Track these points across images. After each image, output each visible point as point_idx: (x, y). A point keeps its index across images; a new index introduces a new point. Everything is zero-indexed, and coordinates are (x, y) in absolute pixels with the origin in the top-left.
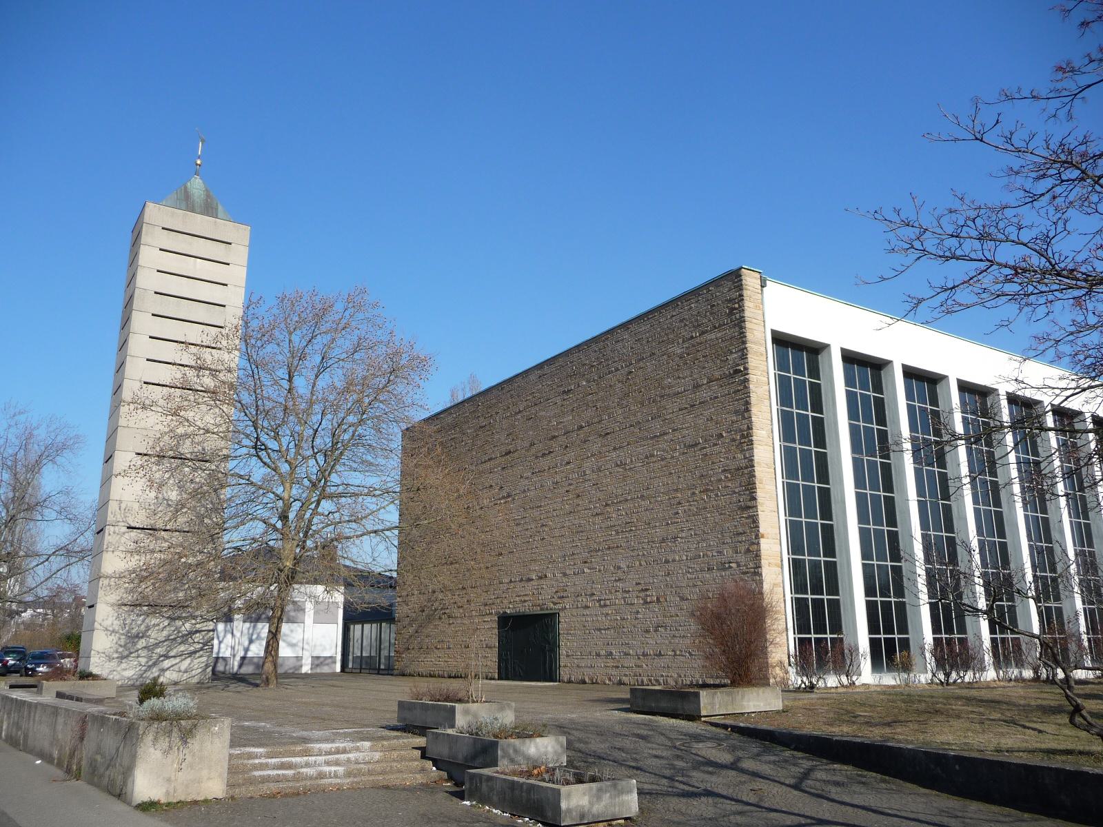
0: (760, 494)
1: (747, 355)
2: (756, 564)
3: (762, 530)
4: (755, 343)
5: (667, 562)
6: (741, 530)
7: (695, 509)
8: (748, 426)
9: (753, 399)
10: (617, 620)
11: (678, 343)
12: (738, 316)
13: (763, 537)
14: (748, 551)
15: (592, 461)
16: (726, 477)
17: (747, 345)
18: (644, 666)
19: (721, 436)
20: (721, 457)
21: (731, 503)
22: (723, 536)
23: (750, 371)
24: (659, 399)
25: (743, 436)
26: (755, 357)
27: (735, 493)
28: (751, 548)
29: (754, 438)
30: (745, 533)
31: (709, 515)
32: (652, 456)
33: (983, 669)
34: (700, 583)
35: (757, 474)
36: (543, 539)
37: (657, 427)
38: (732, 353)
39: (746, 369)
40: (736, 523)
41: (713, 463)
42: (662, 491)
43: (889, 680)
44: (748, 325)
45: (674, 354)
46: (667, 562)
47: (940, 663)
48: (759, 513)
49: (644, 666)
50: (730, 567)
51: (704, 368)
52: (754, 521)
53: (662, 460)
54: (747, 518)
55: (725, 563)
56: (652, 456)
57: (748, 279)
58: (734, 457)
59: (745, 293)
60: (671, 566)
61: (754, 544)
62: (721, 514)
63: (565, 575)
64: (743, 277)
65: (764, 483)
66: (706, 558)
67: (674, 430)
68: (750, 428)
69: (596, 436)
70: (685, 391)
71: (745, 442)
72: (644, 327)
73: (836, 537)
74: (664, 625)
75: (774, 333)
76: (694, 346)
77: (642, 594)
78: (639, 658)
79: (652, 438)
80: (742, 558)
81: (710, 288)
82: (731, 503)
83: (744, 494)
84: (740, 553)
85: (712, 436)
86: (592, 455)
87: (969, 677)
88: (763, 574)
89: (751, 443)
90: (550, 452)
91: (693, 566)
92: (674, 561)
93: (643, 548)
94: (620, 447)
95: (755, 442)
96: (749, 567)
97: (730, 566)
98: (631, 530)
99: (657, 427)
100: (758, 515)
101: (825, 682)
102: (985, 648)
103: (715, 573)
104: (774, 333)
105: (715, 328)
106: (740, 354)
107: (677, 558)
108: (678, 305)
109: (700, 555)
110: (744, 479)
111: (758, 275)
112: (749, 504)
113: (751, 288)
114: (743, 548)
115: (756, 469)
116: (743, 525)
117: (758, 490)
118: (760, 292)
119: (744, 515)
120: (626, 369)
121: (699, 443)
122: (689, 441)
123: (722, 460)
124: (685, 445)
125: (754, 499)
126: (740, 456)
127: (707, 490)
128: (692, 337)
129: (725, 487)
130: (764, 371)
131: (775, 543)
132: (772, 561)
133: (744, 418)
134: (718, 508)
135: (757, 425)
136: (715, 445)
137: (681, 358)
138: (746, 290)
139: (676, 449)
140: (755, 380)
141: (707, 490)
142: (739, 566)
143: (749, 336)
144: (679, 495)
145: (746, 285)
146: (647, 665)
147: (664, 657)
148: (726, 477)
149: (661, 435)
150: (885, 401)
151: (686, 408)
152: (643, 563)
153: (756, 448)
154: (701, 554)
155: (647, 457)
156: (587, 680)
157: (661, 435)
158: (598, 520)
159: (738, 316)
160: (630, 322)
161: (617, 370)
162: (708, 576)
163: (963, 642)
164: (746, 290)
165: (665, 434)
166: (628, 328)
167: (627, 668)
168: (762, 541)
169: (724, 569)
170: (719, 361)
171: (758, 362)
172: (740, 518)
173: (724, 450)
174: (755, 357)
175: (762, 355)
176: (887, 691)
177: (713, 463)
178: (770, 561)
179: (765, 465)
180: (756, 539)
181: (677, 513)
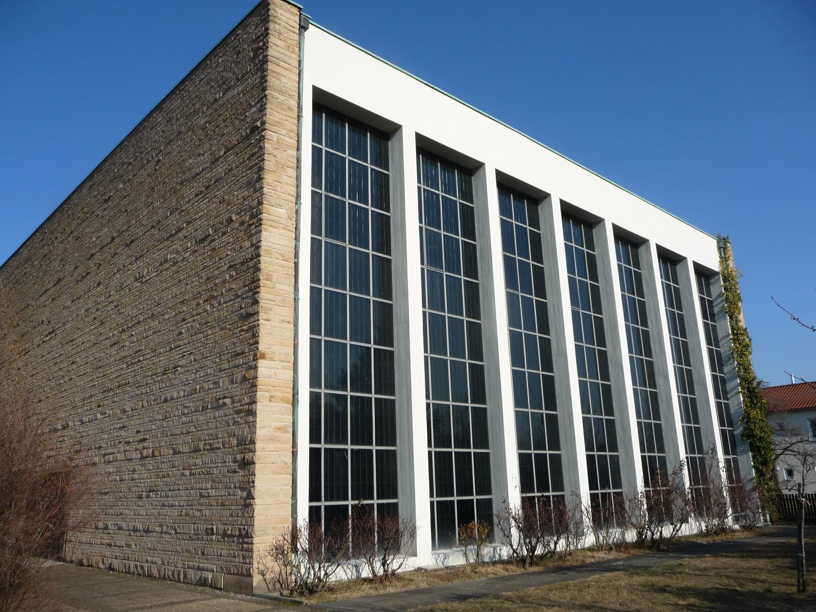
0: (264, 295)
1: (266, 104)
2: (250, 397)
3: (262, 347)
4: (281, 92)
5: (166, 401)
6: (239, 350)
7: (198, 326)
8: (258, 200)
9: (269, 164)
10: (116, 480)
11: (203, 112)
12: (261, 56)
13: (263, 356)
14: (245, 379)
15: (117, 278)
16: (231, 276)
17: (267, 92)
18: (133, 546)
19: (230, 220)
20: (228, 250)
21: (232, 312)
22: (221, 360)
23: (267, 126)
24: (178, 187)
25: (252, 216)
26: (279, 110)
27: (238, 296)
28: (247, 375)
29: (264, 216)
30: (243, 353)
31: (210, 332)
32: (166, 261)
33: (579, 534)
34: (193, 429)
35: (262, 266)
36: (71, 379)
37: (174, 221)
38: (251, 107)
39: (263, 123)
40: (235, 340)
41: (220, 259)
42: (170, 305)
43: (456, 558)
44: (270, 66)
45: (198, 127)
46: (166, 401)
47: (528, 529)
48: (261, 321)
49: (133, 546)
50: (224, 404)
51: (223, 135)
52: (254, 333)
53: (175, 264)
54: (247, 331)
55: (219, 399)
56: (166, 261)
57: (279, 11)
58: (241, 247)
59: (271, 26)
60: (167, 407)
61: (250, 368)
62: (222, 329)
63: (82, 422)
64: (271, 7)
65: (274, 279)
66: (202, 393)
67: (188, 223)
68: (260, 203)
69: (124, 247)
70: (203, 170)
71: (253, 224)
72: (176, 103)
73: (396, 368)
74: (155, 488)
75: (317, 92)
76: (216, 110)
77: (140, 446)
78: (130, 535)
79: (168, 238)
80: (236, 390)
81: (238, 33)
82: (232, 312)
83: (247, 297)
84: (236, 383)
85: (222, 223)
86: (118, 271)
87: (561, 545)
88: (257, 412)
89: (259, 223)
90: (88, 274)
91: (188, 405)
92: (172, 399)
93: (147, 384)
94: (141, 256)
95: (264, 222)
96: (243, 402)
97: (224, 402)
98: (139, 361)
99: (174, 221)
100: (258, 325)
101: (358, 571)
102: (583, 509)
103: (210, 414)
104: (317, 92)
105: (238, 80)
106: (259, 105)
107: (175, 395)
108: (207, 65)
109: (196, 389)
110: (248, 276)
111: (296, 11)
112: (250, 310)
113: (283, 24)
114: (238, 376)
115: (262, 259)
116: (242, 342)
117: (262, 290)
118: (298, 32)
119: (244, 328)
120: (156, 159)
121: (210, 235)
122: (200, 235)
123: (229, 253)
124: (196, 240)
125: (256, 302)
126: (247, 244)
127: (212, 297)
128: (216, 100)
129: (229, 290)
130: (291, 131)
131: (284, 368)
132: (277, 394)
133: (256, 191)
134: (219, 320)
135: (270, 199)
136: (224, 233)
137: (203, 129)
138: (275, 22)
139: (187, 248)
140: (275, 140)
141: (212, 297)
142: (233, 402)
143: (271, 80)
144: (185, 309)
145: (275, 17)
146: (136, 545)
147: (151, 534)
148: (231, 276)
149: (176, 233)
150: (475, 211)
151: (201, 192)
152: (145, 404)
153: (266, 230)
154: (198, 387)
155: (161, 265)
156: (85, 561)
157: (176, 233)
158: (113, 350)
159: (261, 56)
160: (164, 101)
161: (148, 162)
162: (202, 418)
163: (560, 500)
164: (275, 22)
165: (180, 230)
166: (162, 109)
167: (119, 547)
168: (261, 363)
169: (218, 408)
170: (237, 122)
171: (281, 116)
172: (240, 332)
173: (232, 240)
174: (279, 110)
175: (290, 109)
176: (453, 572)
177: (220, 259)
178: (272, 393)
179: (278, 256)
180: (254, 360)
181: (180, 333)
